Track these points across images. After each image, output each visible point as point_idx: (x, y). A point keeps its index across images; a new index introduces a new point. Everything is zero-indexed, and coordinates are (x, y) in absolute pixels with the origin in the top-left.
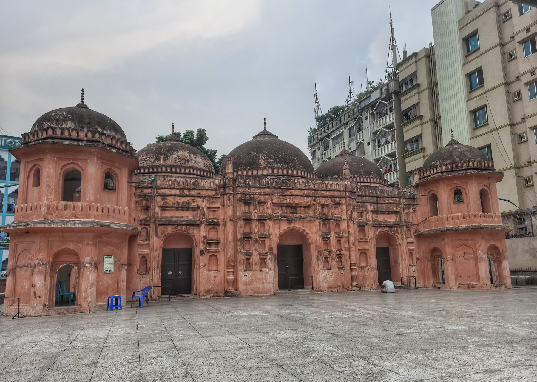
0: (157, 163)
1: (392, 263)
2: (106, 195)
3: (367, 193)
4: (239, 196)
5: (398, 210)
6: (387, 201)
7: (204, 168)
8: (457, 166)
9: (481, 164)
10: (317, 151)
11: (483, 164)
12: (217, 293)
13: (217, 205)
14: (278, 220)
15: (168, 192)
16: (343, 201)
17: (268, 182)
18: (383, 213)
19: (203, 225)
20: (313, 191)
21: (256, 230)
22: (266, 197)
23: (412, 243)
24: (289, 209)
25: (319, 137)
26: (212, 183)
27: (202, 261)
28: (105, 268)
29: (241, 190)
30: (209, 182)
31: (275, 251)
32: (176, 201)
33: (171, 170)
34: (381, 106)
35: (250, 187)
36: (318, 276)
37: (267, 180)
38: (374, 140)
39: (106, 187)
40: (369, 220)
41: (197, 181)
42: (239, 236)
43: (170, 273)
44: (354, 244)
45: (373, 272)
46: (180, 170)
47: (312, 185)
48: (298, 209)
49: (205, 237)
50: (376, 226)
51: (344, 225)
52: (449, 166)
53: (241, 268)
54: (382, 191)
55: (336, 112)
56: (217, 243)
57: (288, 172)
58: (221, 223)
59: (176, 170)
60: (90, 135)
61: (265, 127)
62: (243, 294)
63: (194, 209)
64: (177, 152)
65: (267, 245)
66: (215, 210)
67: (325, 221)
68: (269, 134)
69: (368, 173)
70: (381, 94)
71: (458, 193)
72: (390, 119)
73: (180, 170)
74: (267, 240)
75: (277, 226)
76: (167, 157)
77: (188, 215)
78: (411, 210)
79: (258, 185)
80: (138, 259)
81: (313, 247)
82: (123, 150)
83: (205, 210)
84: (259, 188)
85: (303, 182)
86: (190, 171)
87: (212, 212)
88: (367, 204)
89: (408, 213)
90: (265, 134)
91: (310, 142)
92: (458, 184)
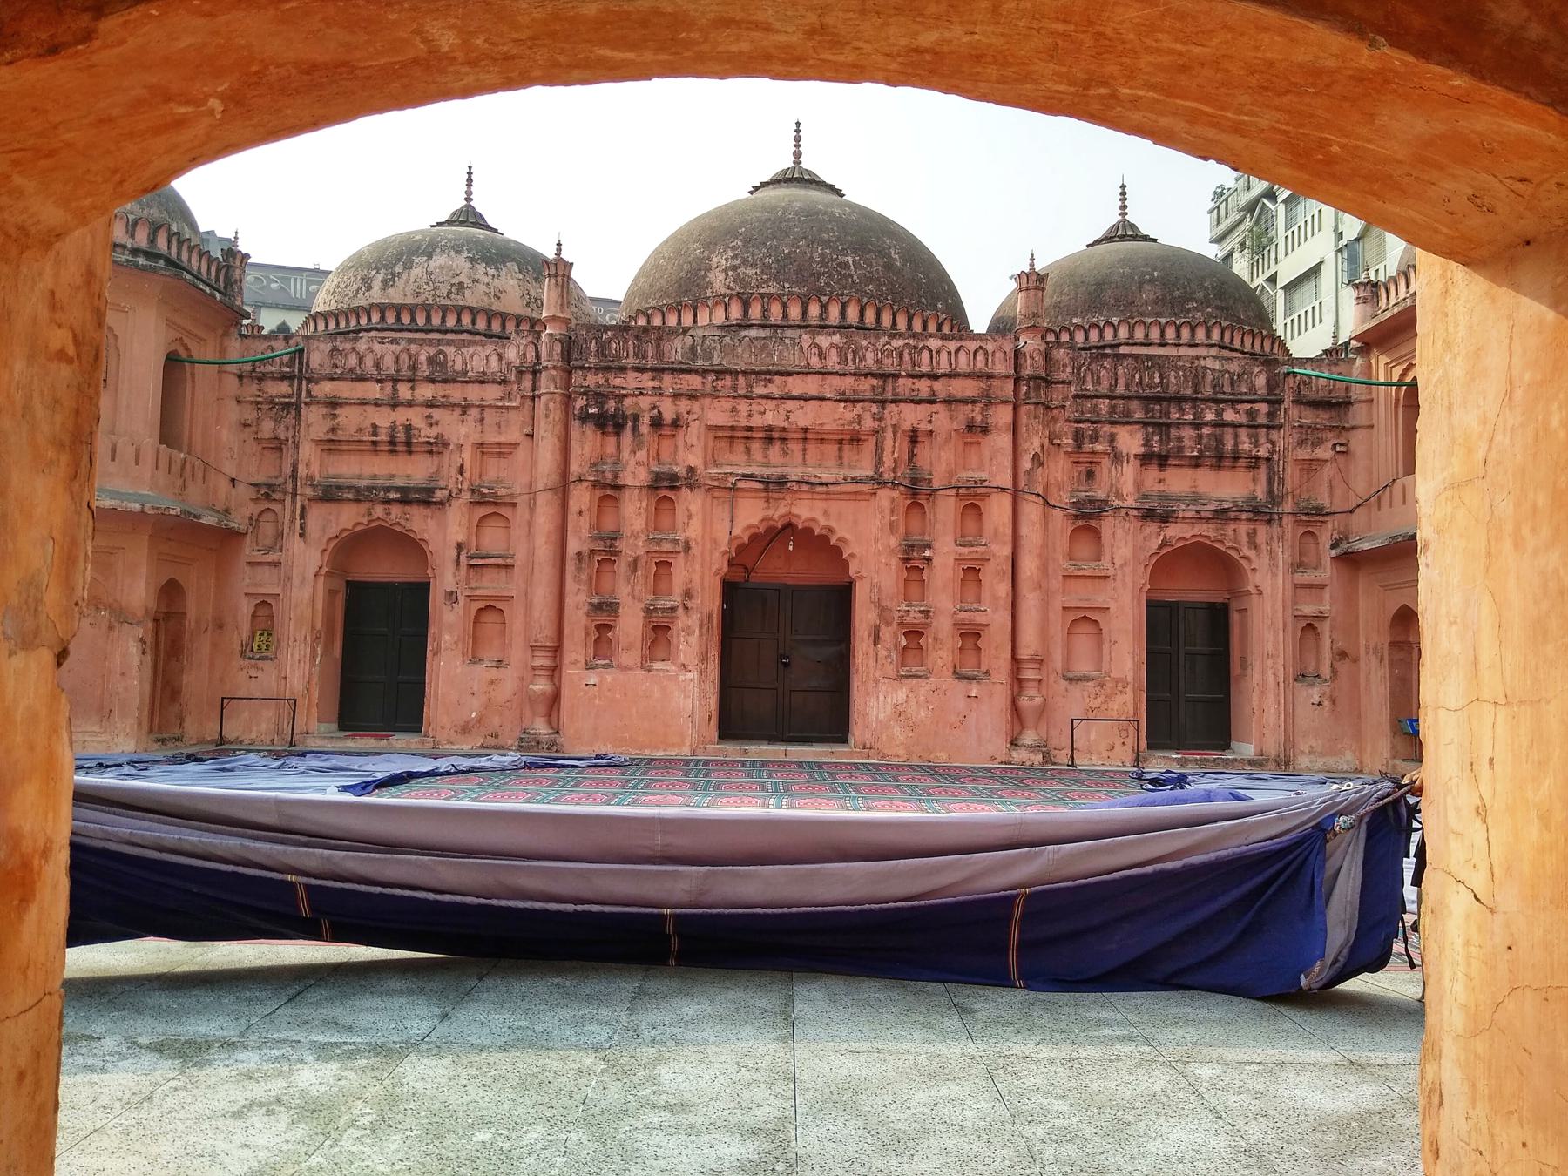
0: (362, 301)
1: (1235, 669)
3: (1121, 382)
4: (580, 402)
5: (1263, 452)
6: (1210, 416)
7: (528, 312)
10: (1236, 255)
12: (495, 735)
13: (513, 434)
14: (728, 491)
15: (345, 390)
17: (693, 349)
19: (455, 502)
20: (875, 382)
21: (639, 524)
22: (684, 405)
23: (1322, 586)
25: (1245, 198)
26: (494, 359)
27: (447, 625)
29: (593, 380)
30: (483, 355)
31: (709, 601)
32: (368, 423)
33: (398, 319)
35: (623, 369)
36: (872, 702)
37: (688, 340)
40: (1119, 496)
41: (441, 352)
45: (1120, 699)
46: (428, 318)
47: (870, 356)
49: (460, 547)
51: (998, 510)
53: (575, 651)
54: (1197, 375)
57: (805, 312)
58: (522, 500)
59: (413, 320)
61: (798, 155)
64: (430, 257)
66: (504, 451)
67: (917, 491)
68: (812, 182)
73: (428, 318)
75: (721, 512)
76: (394, 275)
78: (1324, 452)
80: (246, 608)
81: (861, 595)
83: (467, 454)
84: (658, 371)
85: (832, 345)
86: (459, 320)
88: (1114, 430)
89: (1310, 467)
90: (798, 177)
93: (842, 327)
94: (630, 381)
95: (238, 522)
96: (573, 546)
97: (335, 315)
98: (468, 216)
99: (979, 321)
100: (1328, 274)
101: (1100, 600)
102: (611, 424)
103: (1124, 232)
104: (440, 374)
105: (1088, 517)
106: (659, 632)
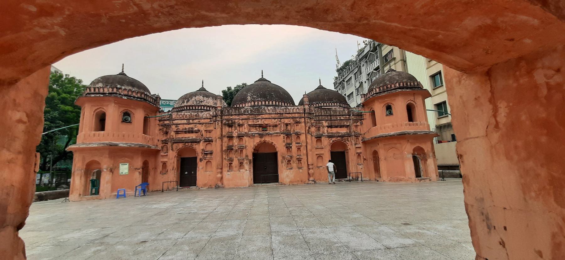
0: (183, 105)
1: (347, 163)
2: (125, 126)
8: (387, 88)
9: (407, 84)
11: (409, 84)
13: (211, 128)
14: (253, 136)
15: (179, 122)
16: (303, 120)
18: (336, 127)
21: (236, 144)
24: (261, 129)
25: (339, 82)
27: (201, 166)
28: (121, 171)
29: (226, 117)
31: (251, 157)
34: (371, 56)
35: (232, 115)
38: (368, 79)
39: (125, 121)
42: (224, 148)
43: (186, 173)
44: (311, 150)
48: (268, 127)
49: (203, 150)
50: (330, 137)
51: (303, 137)
52: (382, 88)
53: (225, 169)
54: (335, 111)
55: (347, 64)
56: (211, 153)
60: (110, 90)
62: (227, 187)
63: (197, 132)
65: (244, 154)
67: (288, 135)
69: (330, 100)
70: (371, 48)
71: (389, 108)
72: (377, 63)
74: (244, 150)
77: (193, 136)
78: (359, 124)
79: (237, 113)
80: (161, 165)
82: (137, 98)
83: (203, 132)
87: (208, 133)
89: (356, 126)
90: (262, 79)
91: (335, 86)
92: (388, 101)
93: (272, 105)
94: (234, 117)
95: (159, 148)
96: (224, 148)
97: (178, 108)
98: (203, 89)
99: (297, 103)
100: (354, 94)
101: (322, 152)
102: (230, 126)
103: (321, 87)
104: (197, 117)
105: (319, 138)
106: (241, 164)
